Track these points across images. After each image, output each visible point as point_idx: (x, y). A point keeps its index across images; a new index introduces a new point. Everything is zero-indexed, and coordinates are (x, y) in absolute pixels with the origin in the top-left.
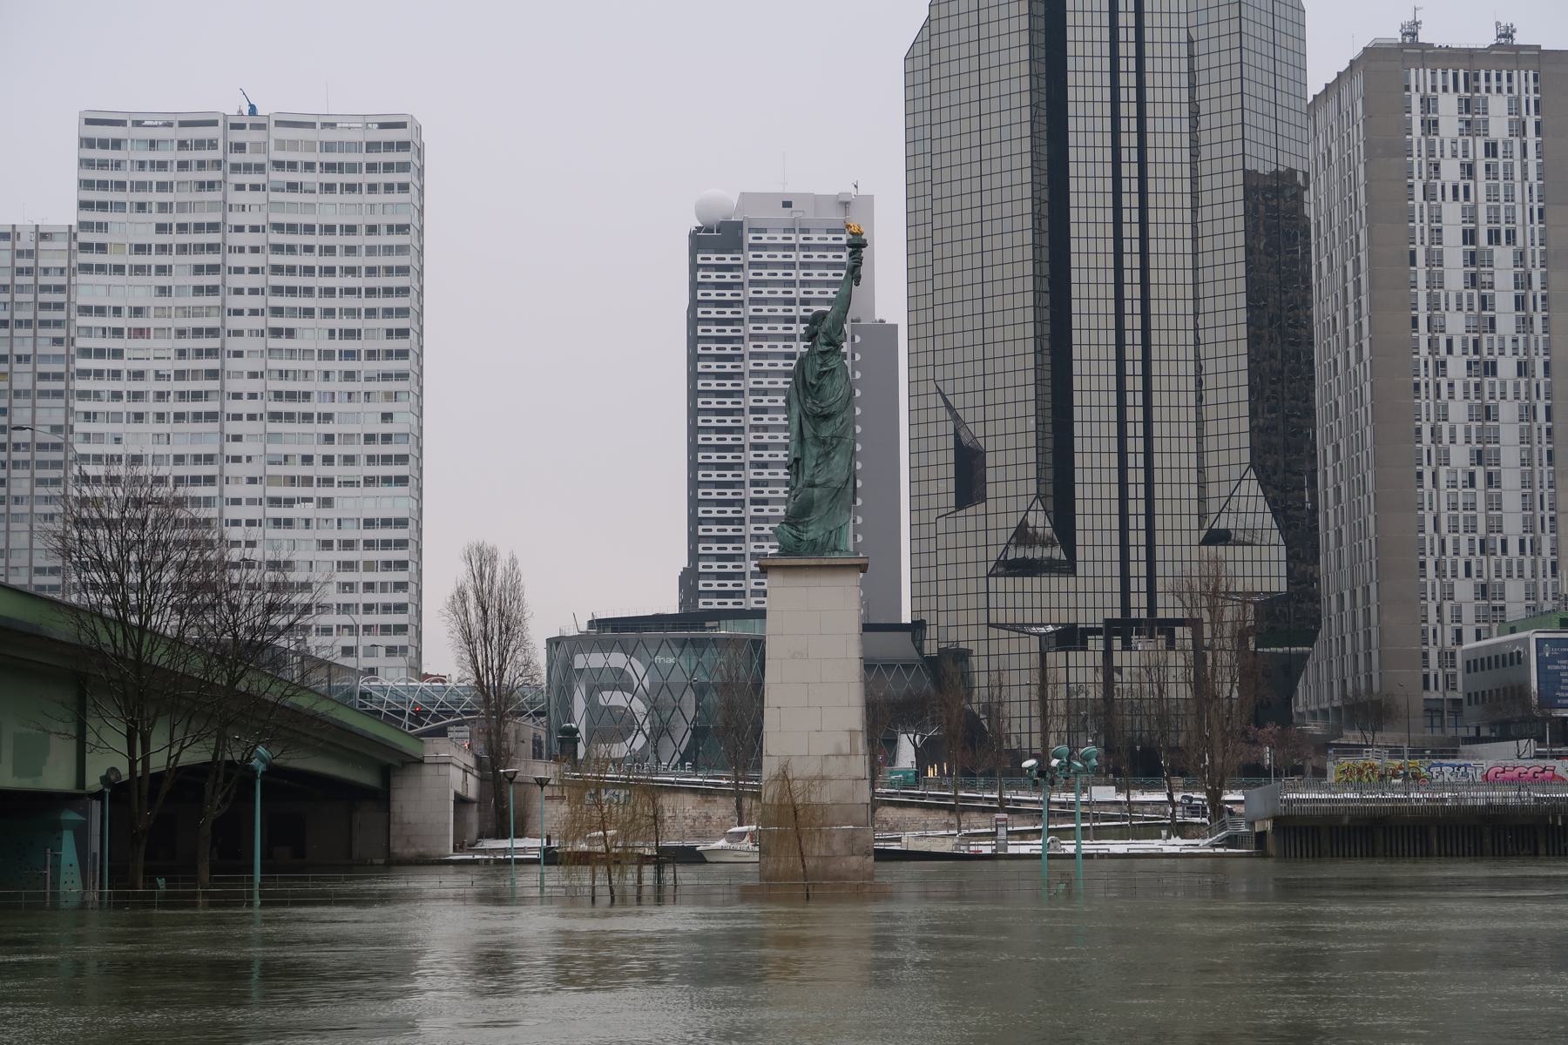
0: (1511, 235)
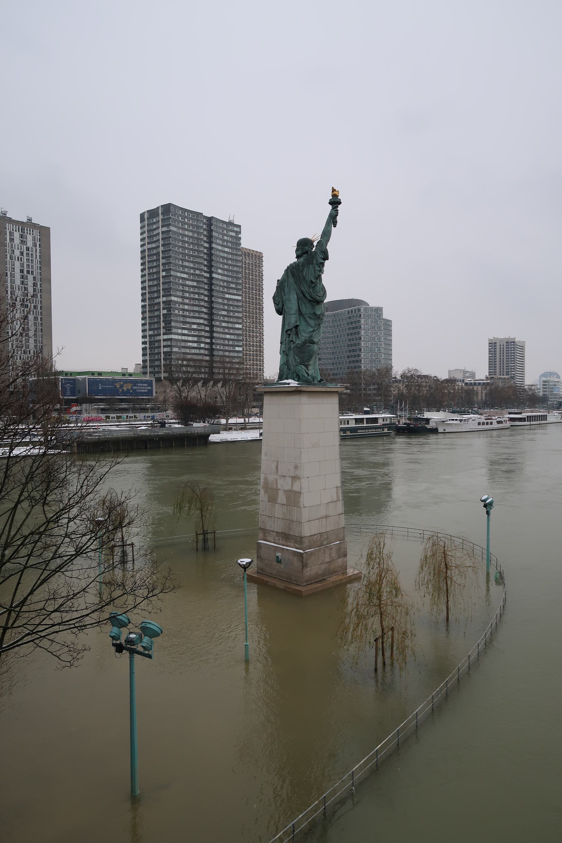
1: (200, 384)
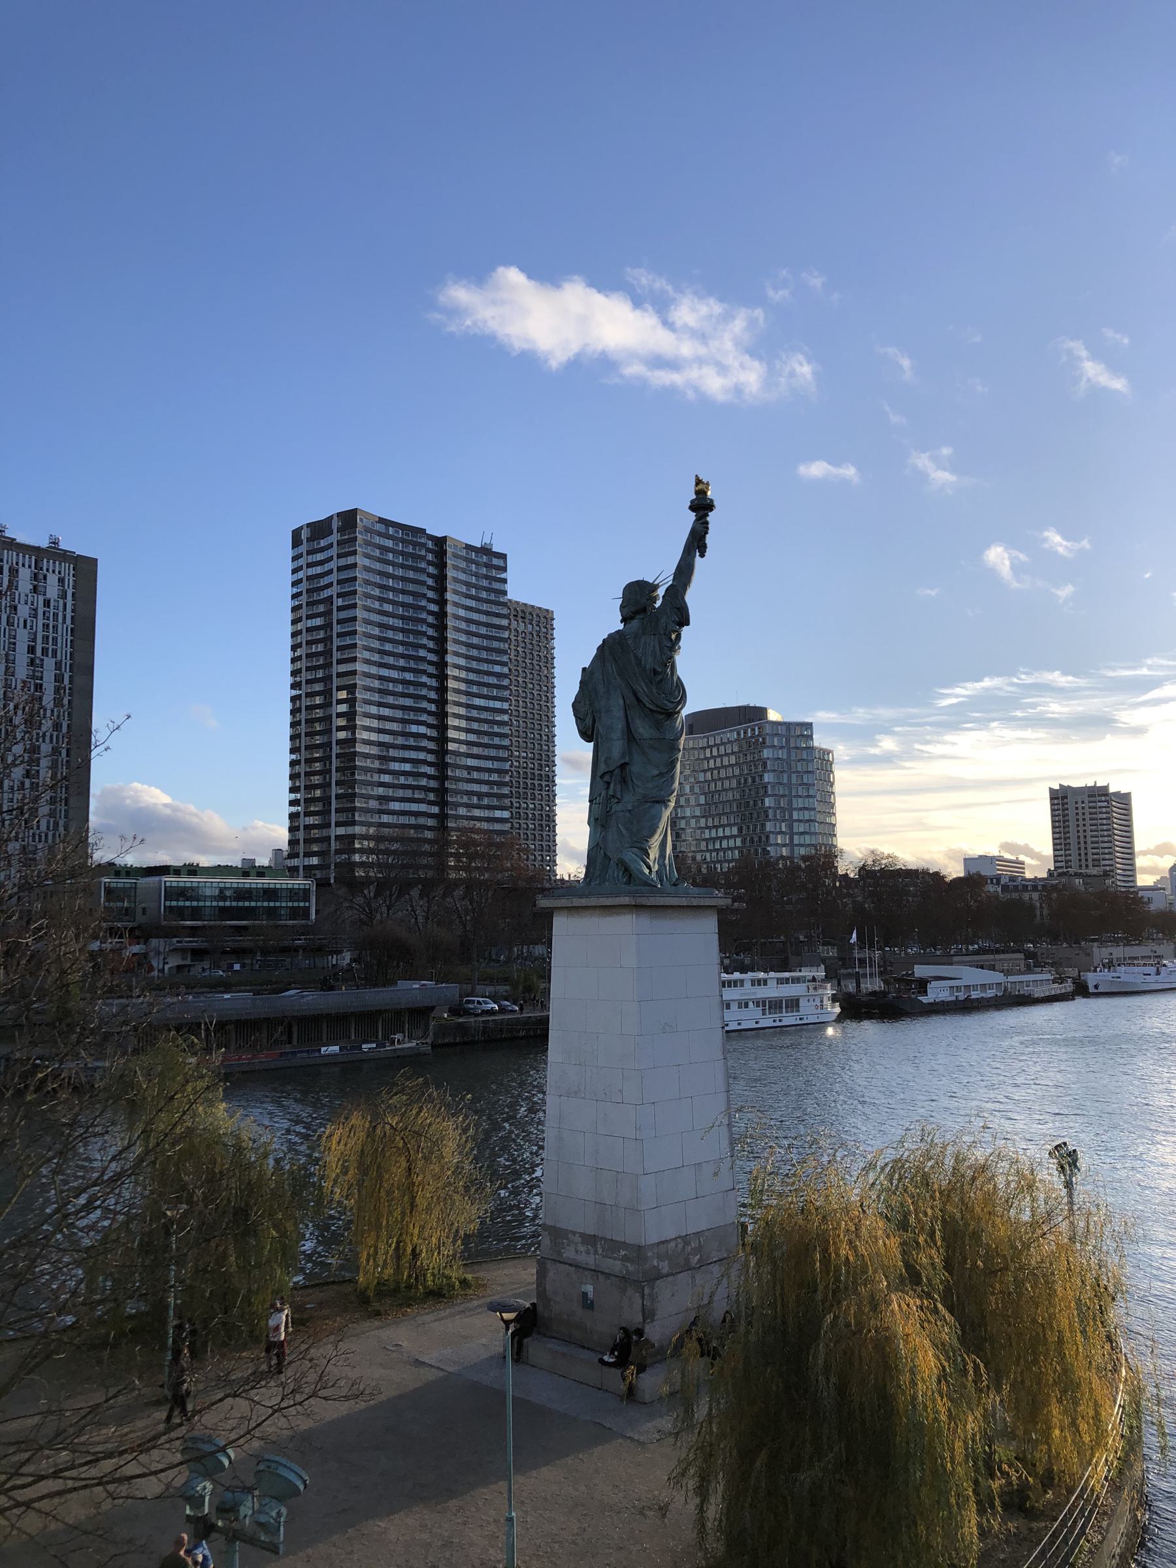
0: (55, 652)
1: (415, 893)
